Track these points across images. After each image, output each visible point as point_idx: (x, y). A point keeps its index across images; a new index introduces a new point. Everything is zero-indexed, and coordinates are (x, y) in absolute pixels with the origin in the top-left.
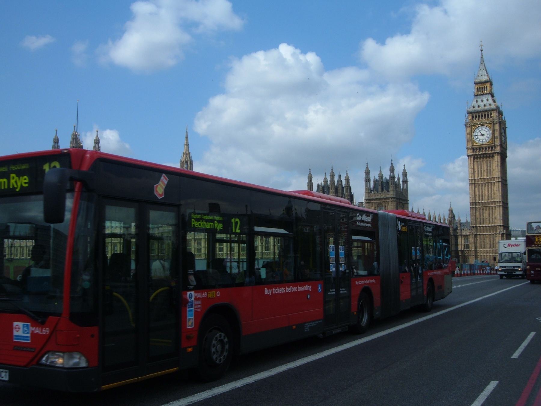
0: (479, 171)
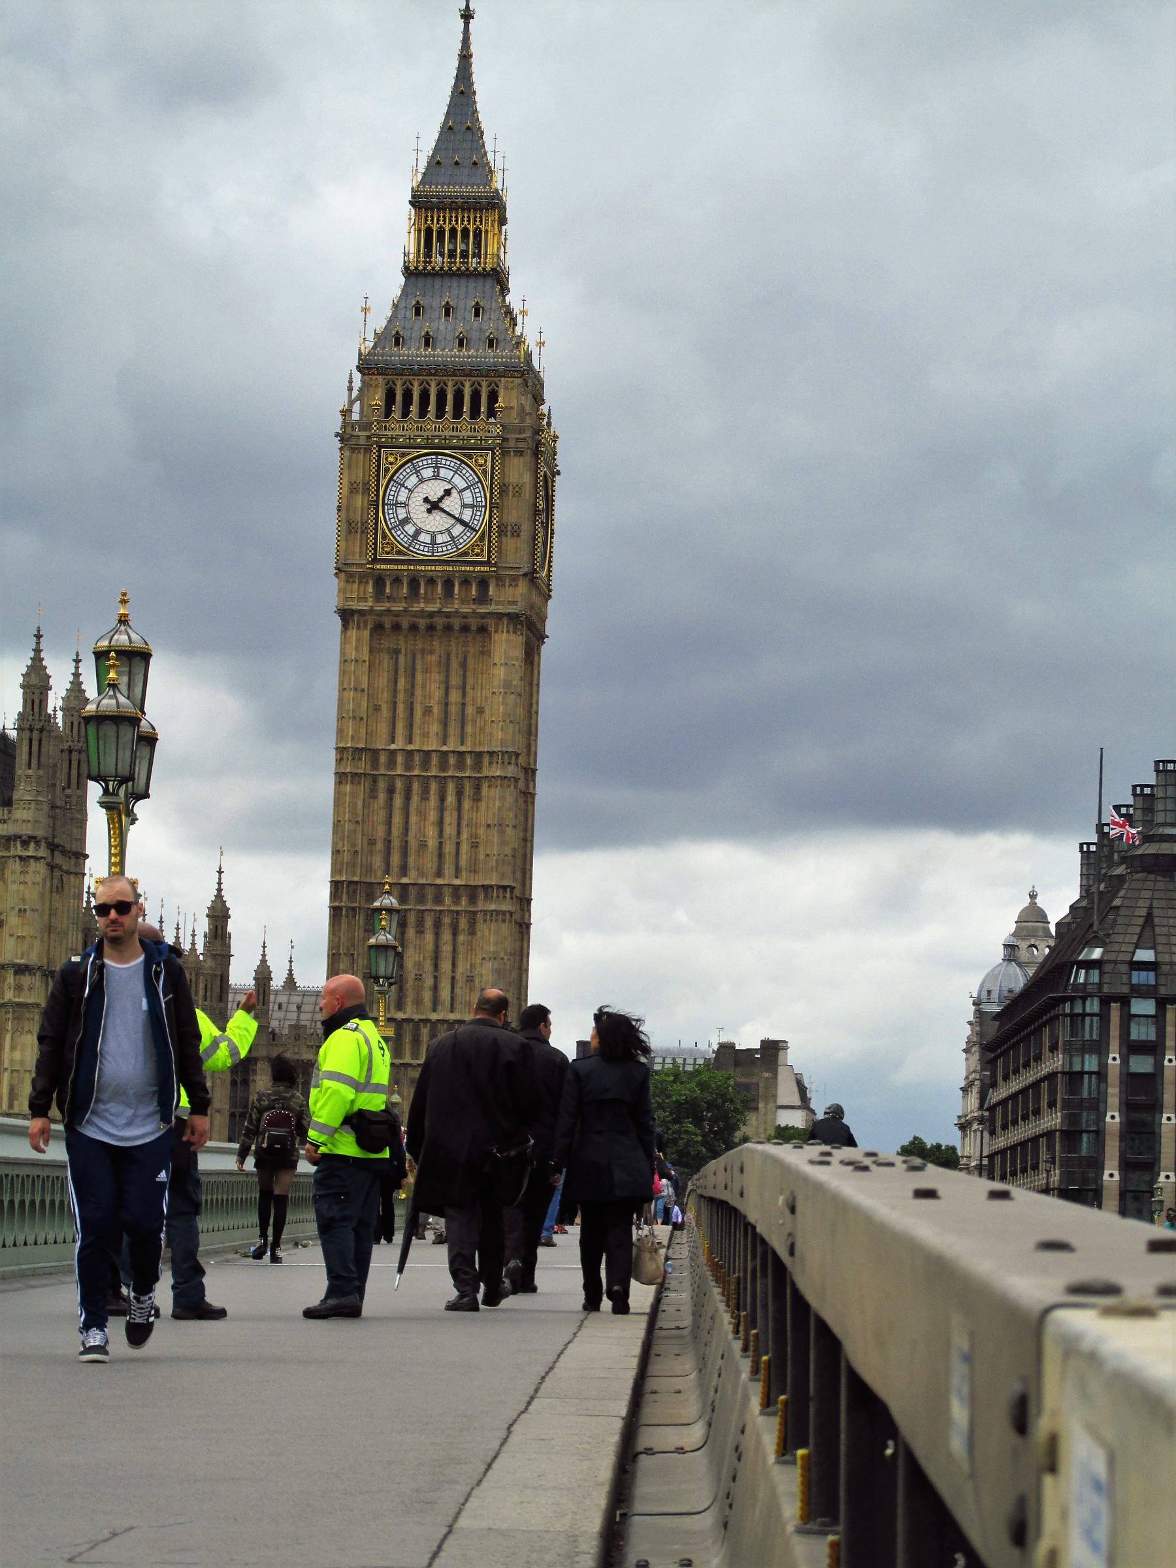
0: (401, 708)
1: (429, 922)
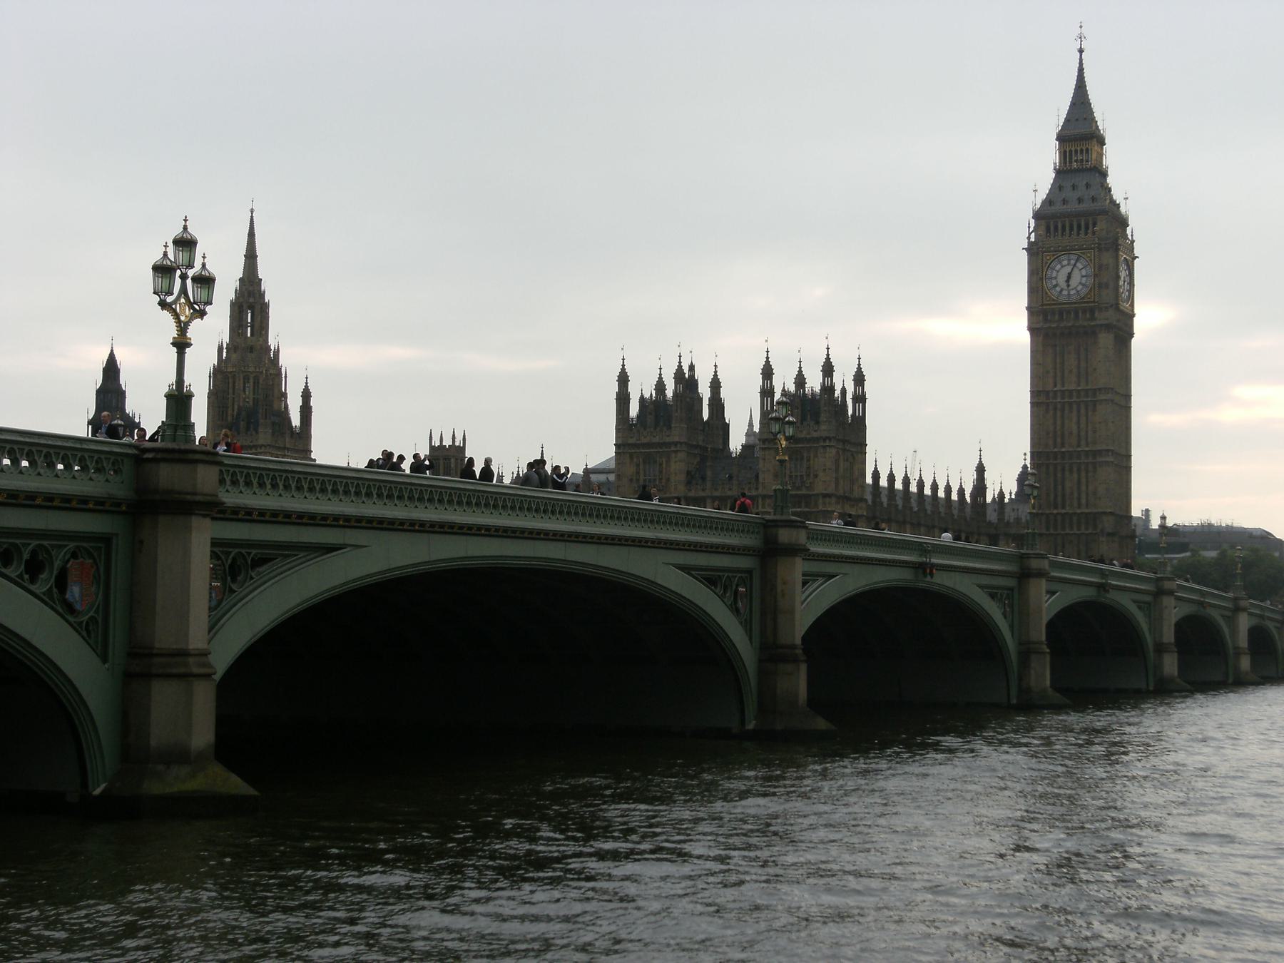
0: (1059, 374)
1: (1075, 469)
